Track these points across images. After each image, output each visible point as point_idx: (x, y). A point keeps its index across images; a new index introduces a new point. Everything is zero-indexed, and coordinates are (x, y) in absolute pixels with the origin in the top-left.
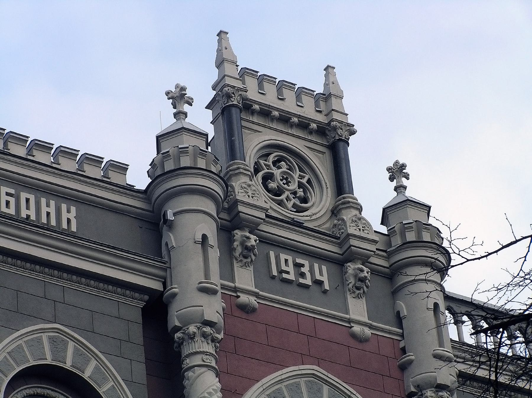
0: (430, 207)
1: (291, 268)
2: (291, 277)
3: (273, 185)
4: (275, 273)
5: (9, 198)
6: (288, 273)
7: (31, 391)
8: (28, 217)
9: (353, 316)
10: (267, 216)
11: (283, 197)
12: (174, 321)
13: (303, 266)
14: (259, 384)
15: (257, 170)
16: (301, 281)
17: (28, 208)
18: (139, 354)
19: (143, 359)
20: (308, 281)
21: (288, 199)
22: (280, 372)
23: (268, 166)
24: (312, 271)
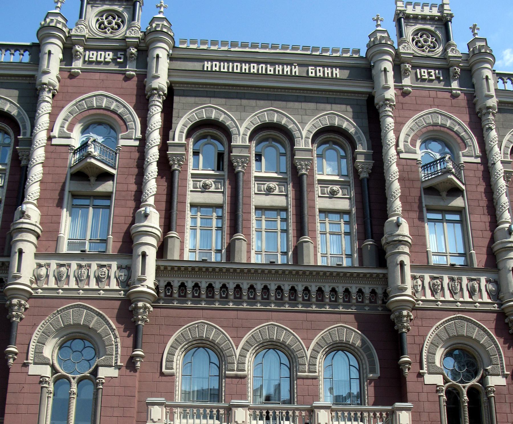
0: (486, 39)
1: (426, 74)
2: (426, 77)
3: (420, 44)
4: (419, 77)
5: (312, 71)
6: (425, 76)
7: (325, 137)
8: (320, 76)
9: (453, 87)
10: (414, 56)
11: (424, 48)
12: (376, 101)
13: (431, 72)
14: (412, 118)
15: (413, 40)
16: (430, 78)
17: (320, 72)
18: (366, 116)
19: (367, 117)
20: (434, 78)
21: (426, 49)
22: (421, 113)
23: (418, 38)
24: (435, 74)
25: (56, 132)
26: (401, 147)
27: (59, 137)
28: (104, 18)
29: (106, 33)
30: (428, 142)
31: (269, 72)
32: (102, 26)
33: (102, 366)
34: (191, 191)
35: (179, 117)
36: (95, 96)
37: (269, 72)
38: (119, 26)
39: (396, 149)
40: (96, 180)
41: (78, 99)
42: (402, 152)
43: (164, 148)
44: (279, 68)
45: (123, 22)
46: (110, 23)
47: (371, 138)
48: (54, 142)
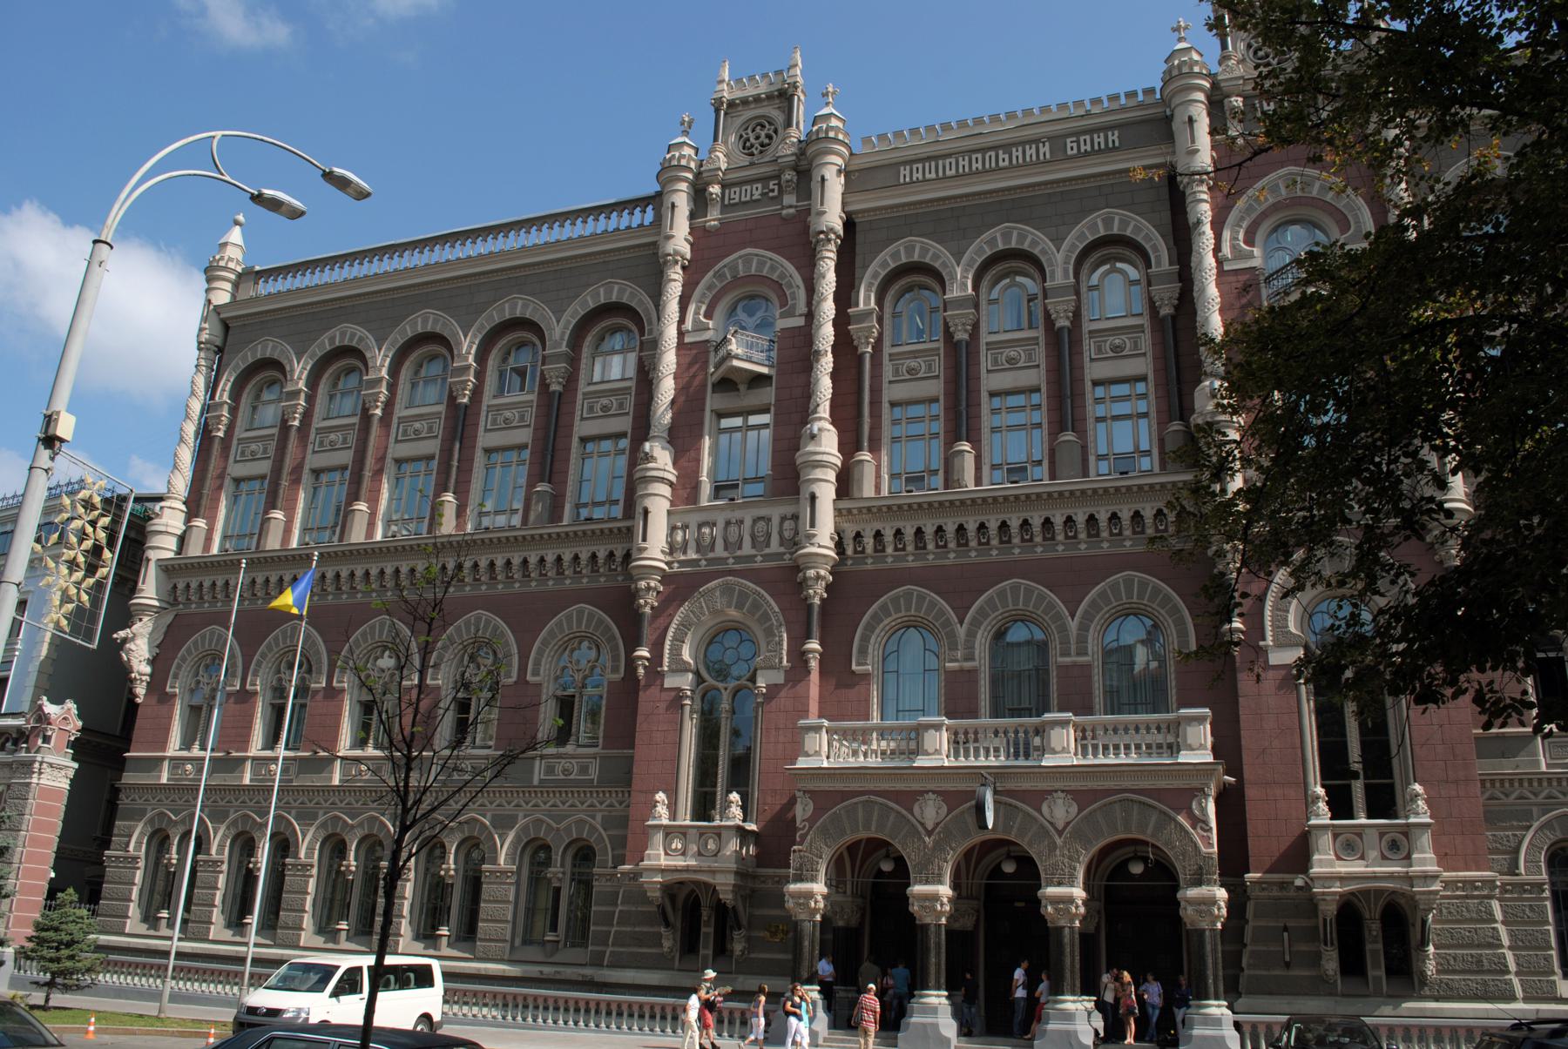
25: (689, 325)
26: (1226, 250)
27: (694, 331)
28: (749, 131)
29: (752, 154)
30: (1280, 230)
31: (1001, 164)
32: (748, 144)
33: (762, 668)
34: (890, 382)
35: (866, 267)
36: (740, 257)
37: (1001, 164)
38: (769, 137)
39: (1215, 256)
40: (749, 388)
41: (717, 268)
42: (1227, 259)
43: (841, 322)
44: (1017, 153)
45: (776, 131)
46: (757, 138)
47: (1176, 243)
48: (687, 340)
